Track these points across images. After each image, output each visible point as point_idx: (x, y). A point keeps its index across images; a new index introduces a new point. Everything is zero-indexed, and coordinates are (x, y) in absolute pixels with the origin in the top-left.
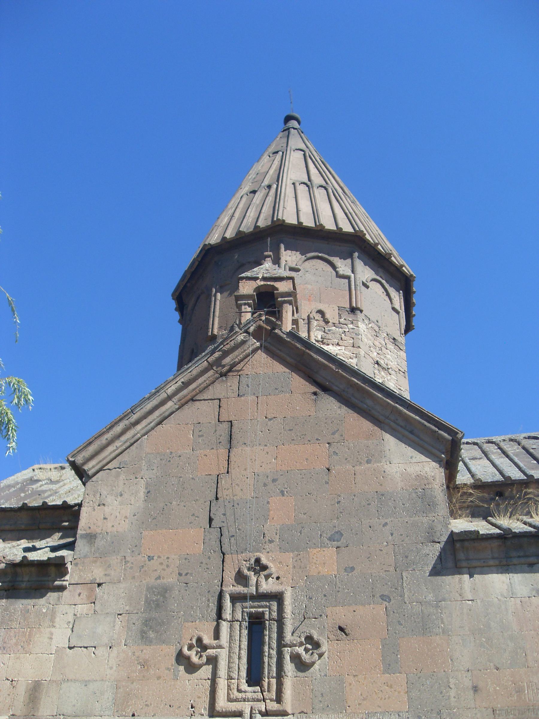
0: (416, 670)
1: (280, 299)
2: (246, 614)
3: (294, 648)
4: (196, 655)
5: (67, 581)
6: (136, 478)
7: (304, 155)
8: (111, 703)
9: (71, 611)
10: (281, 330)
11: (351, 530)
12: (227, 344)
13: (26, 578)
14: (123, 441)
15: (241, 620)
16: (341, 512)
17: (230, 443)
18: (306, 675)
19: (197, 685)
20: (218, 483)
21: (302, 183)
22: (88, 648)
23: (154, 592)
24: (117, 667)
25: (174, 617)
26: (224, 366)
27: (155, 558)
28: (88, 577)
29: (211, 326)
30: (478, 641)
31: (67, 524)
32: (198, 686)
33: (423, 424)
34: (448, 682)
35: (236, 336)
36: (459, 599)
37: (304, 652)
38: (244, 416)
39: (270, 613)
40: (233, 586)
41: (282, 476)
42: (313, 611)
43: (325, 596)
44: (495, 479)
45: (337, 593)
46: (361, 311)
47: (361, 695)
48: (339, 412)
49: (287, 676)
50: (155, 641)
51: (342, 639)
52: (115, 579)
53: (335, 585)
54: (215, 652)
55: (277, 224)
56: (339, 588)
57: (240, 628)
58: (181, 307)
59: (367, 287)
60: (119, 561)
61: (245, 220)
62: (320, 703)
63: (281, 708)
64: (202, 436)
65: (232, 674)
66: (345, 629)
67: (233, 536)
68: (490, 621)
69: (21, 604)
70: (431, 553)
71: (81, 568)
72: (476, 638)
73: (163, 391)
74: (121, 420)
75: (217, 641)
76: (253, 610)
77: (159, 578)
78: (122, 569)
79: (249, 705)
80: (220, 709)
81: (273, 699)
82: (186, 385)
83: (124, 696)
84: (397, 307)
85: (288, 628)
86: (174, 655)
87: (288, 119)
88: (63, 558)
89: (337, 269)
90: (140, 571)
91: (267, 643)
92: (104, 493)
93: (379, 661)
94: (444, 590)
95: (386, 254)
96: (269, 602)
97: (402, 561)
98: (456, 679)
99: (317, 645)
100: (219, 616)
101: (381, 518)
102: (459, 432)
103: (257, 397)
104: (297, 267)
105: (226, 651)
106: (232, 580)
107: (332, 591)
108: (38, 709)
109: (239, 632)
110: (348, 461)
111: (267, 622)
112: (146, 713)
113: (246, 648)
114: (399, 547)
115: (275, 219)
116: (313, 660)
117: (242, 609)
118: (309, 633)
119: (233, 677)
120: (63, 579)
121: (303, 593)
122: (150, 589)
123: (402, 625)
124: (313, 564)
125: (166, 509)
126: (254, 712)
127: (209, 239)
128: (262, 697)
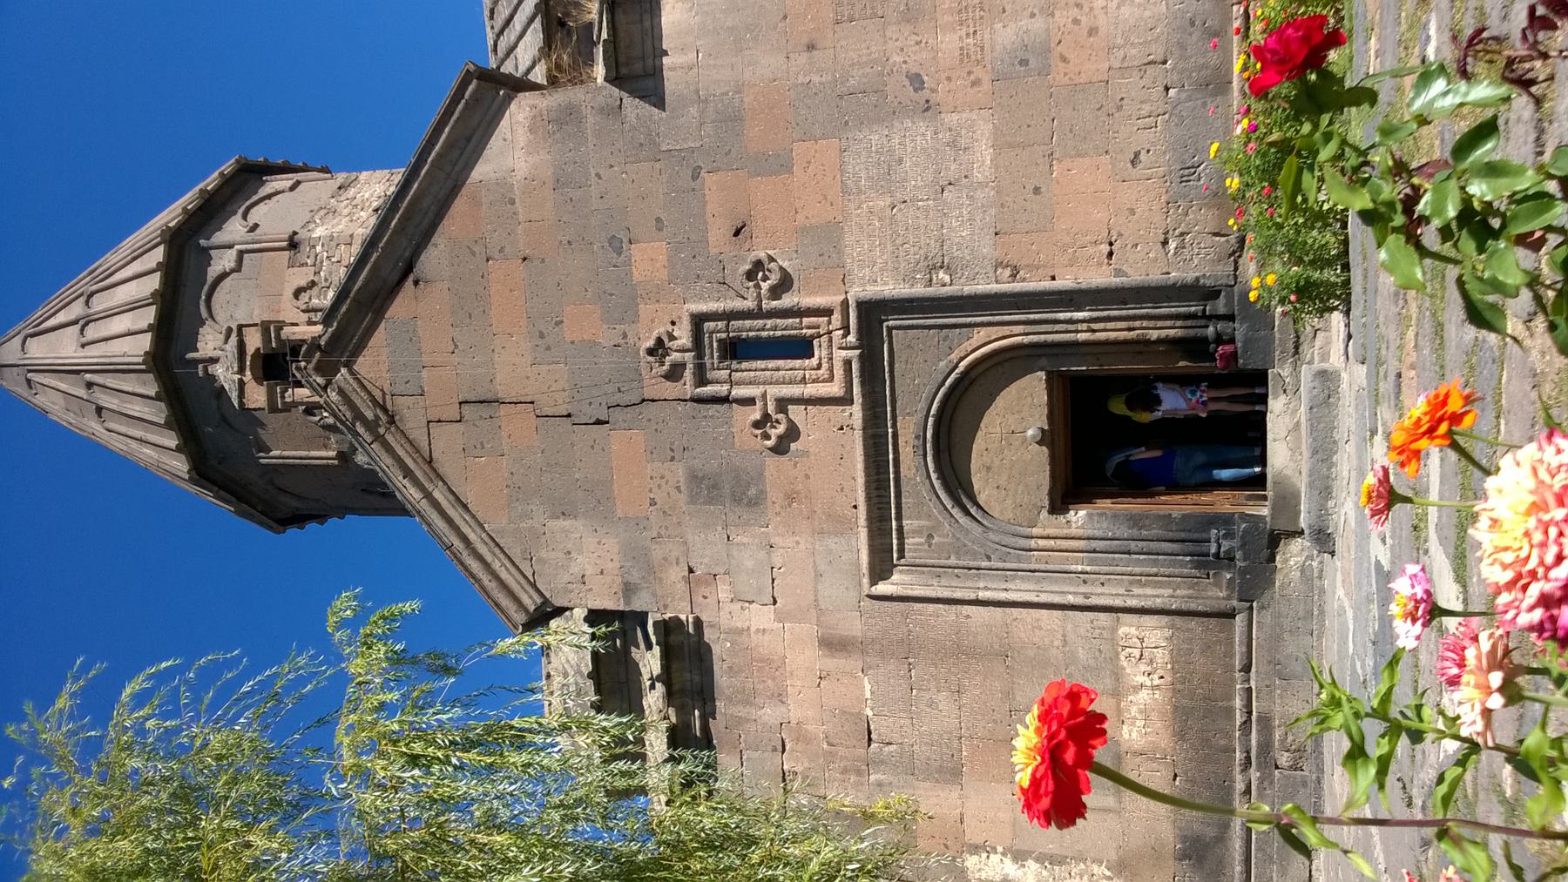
1: (274, 345)
5: (687, 617)
7: (32, 336)
10: (320, 337)
13: (688, 675)
16: (583, 239)
20: (547, 416)
21: (82, 334)
26: (377, 417)
28: (681, 587)
31: (618, 641)
33: (456, 122)
37: (768, 282)
39: (719, 332)
40: (685, 384)
43: (694, 257)
44: (540, 28)
46: (295, 233)
50: (761, 487)
55: (152, 364)
58: (299, 519)
59: (256, 226)
64: (482, 443)
65: (799, 379)
69: (722, 679)
76: (716, 355)
77: (678, 488)
82: (408, 473)
84: (289, 184)
85: (739, 304)
86: (777, 457)
88: (655, 624)
89: (227, 270)
92: (566, 578)
99: (758, 265)
100: (725, 400)
104: (224, 332)
108: (854, 637)
111: (731, 335)
115: (143, 367)
122: (693, 500)
126: (844, 345)
127: (180, 474)
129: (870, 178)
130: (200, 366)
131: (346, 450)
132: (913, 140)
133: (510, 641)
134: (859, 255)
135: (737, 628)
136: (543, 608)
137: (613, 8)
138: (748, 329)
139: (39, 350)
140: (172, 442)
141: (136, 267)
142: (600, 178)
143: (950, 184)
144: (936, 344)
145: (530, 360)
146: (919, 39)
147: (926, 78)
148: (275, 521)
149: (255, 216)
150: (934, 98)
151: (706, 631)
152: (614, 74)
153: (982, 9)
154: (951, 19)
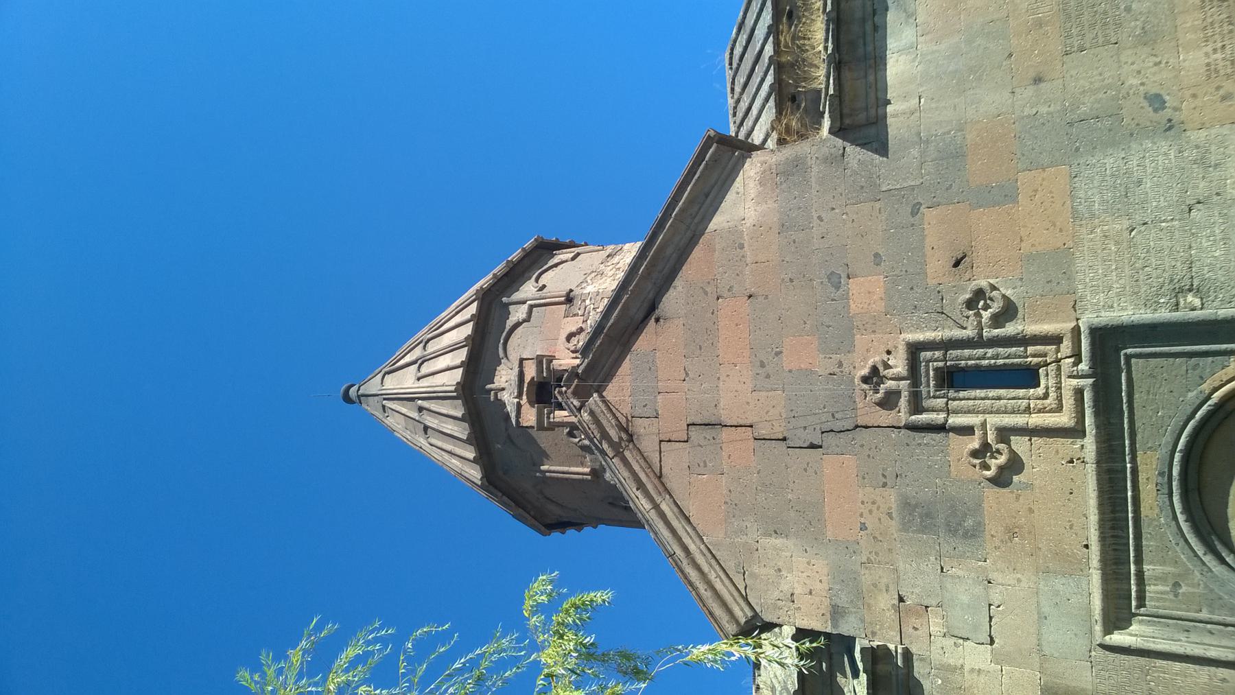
1: (545, 375)
2: (938, 393)
3: (983, 324)
4: (996, 459)
5: (896, 647)
6: (757, 550)
7: (389, 373)
9: (939, 642)
10: (578, 366)
11: (827, 261)
12: (593, 433)
15: (946, 399)
16: (804, 276)
17: (715, 425)
19: (1040, 456)
20: (764, 439)
22: (991, 615)
23: (909, 521)
24: (1017, 573)
28: (891, 615)
29: (581, 476)
30: (974, 85)
31: (824, 664)
33: (697, 180)
34: (1029, 116)
35: (583, 422)
37: (989, 310)
39: (936, 360)
40: (899, 412)
43: (912, 289)
46: (571, 291)
48: (680, 288)
50: (979, 518)
55: (461, 392)
56: (901, 270)
57: (958, 400)
58: (562, 525)
59: (544, 286)
60: (867, 572)
61: (456, 434)
63: (1069, 335)
64: (705, 462)
65: (1022, 408)
67: (833, 415)
70: (858, 157)
72: (970, 87)
73: (647, 515)
76: (932, 383)
77: (890, 515)
78: (878, 567)
79: (1065, 382)
82: (640, 486)
83: (1059, 561)
84: (571, 255)
85: (957, 333)
86: (997, 489)
87: (347, 398)
88: (863, 650)
89: (520, 320)
91: (978, 361)
92: (776, 594)
99: (979, 293)
100: (941, 428)
103: (659, 393)
105: (990, 417)
114: (848, 199)
115: (455, 394)
116: (1000, 297)
117: (930, 398)
119: (1027, 406)
120: (894, 654)
121: (909, 318)
122: (905, 527)
124: (870, 308)
126: (1075, 373)
127: (475, 481)
128: (1053, 364)
129: (1103, 202)
130: (492, 393)
131: (597, 467)
132: (1153, 161)
133: (705, 648)
136: (753, 622)
137: (840, 67)
138: (967, 358)
139: (393, 384)
140: (471, 455)
142: (822, 221)
143: (1199, 203)
144: (1184, 373)
145: (750, 386)
146: (1158, 60)
147: (1167, 98)
148: (544, 526)
150: (1177, 117)
151: (916, 664)
152: (838, 124)
153: (1231, 24)
154: (1193, 36)
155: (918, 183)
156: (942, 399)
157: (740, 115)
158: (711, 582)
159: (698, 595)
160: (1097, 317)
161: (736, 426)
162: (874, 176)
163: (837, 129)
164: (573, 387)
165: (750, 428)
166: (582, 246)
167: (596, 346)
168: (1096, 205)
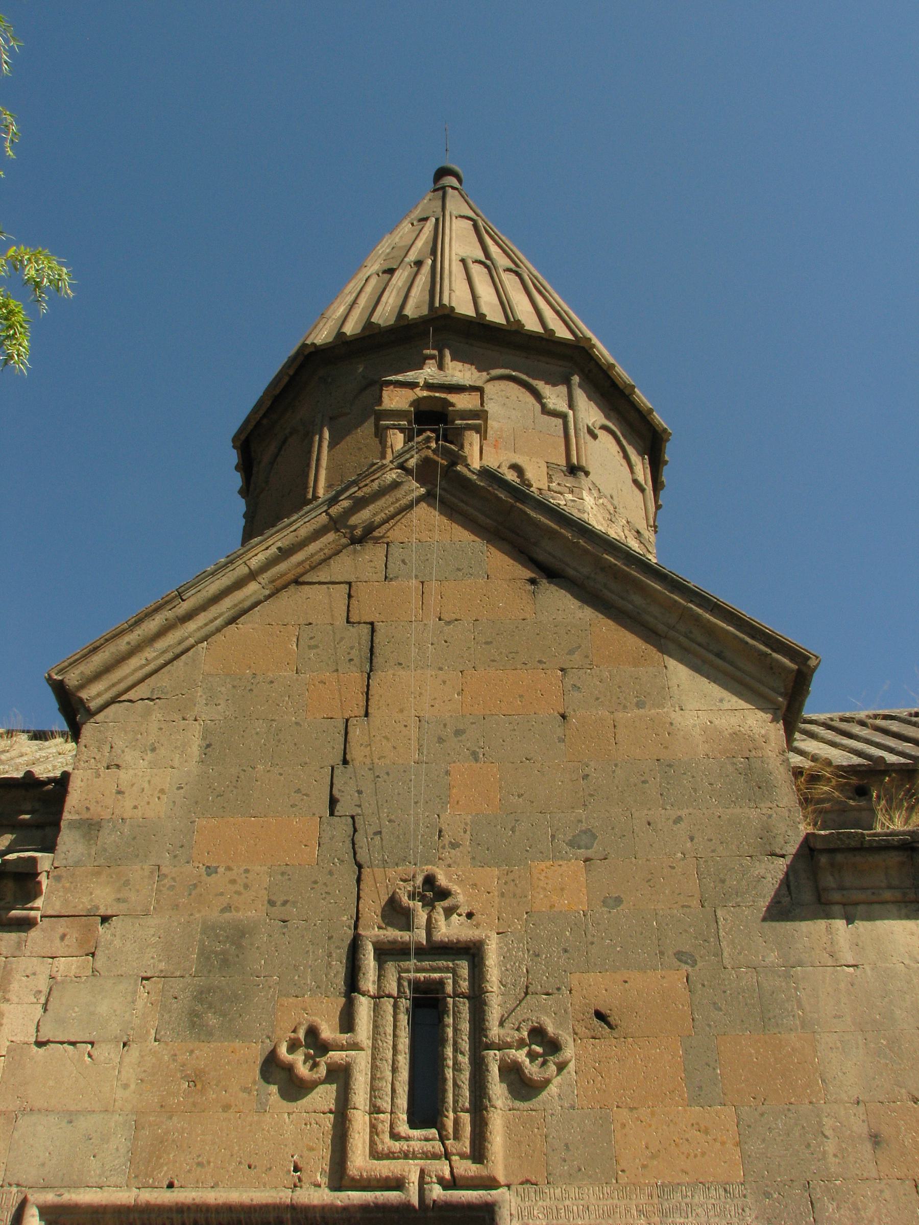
0: (754, 1098)
1: (457, 422)
2: (406, 984)
3: (508, 1050)
4: (305, 1062)
5: (37, 909)
6: (184, 719)
8: (122, 1160)
9: (43, 969)
10: (467, 466)
11: (613, 828)
12: (366, 485)
14: (160, 649)
15: (396, 995)
16: (591, 795)
17: (371, 663)
18: (531, 1106)
19: (306, 1124)
20: (346, 733)
23: (217, 936)
24: (137, 1084)
25: (259, 985)
27: (221, 870)
28: (82, 903)
29: (312, 484)
30: (872, 1045)
32: (309, 1126)
33: (742, 640)
34: (820, 1124)
35: (382, 472)
36: (830, 962)
37: (528, 1060)
38: (397, 615)
39: (455, 982)
40: (380, 928)
41: (474, 725)
42: (542, 979)
43: (566, 951)
45: (590, 946)
46: (587, 474)
47: (647, 1148)
48: (579, 614)
49: (496, 1108)
51: (602, 1035)
52: (139, 909)
53: (585, 931)
54: (345, 1056)
55: (440, 313)
56: (594, 936)
58: (247, 466)
59: (595, 437)
60: (147, 873)
61: (379, 309)
62: (563, 1163)
63: (485, 1173)
64: (317, 647)
65: (379, 1102)
66: (609, 1016)
68: (893, 1007)
70: (769, 875)
71: (68, 885)
73: (241, 562)
74: (157, 610)
75: (349, 1034)
76: (421, 976)
77: (227, 908)
78: (152, 889)
79: (417, 1165)
80: (356, 1173)
81: (467, 1153)
82: (285, 553)
83: (152, 1145)
84: (641, 479)
85: (494, 1013)
86: (259, 1061)
87: (442, 172)
88: (34, 860)
90: (190, 895)
91: (451, 1041)
92: (119, 744)
93: (678, 1080)
94: (800, 946)
95: (626, 387)
96: (453, 961)
97: (715, 888)
98: (836, 1118)
99: (553, 1046)
100: (352, 985)
101: (668, 808)
102: (811, 656)
103: (422, 583)
105: (367, 1055)
106: (377, 916)
107: (580, 942)
109: (392, 1019)
110: (601, 702)
111: (450, 1000)
112: (197, 1181)
113: (407, 1051)
115: (437, 304)
116: (546, 1076)
117: (399, 973)
118: (537, 1023)
119: (382, 1108)
120: (29, 905)
121: (521, 945)
122: (209, 929)
123: (720, 1010)
125: (243, 777)
126: (428, 1179)
127: (312, 337)
128: (442, 1149)
130: (436, 352)
134: (567, 1208)
135: (10, 983)
141: (548, 314)
149: (605, 439)
151: (13, 936)
152: (819, 846)
155: (726, 962)
156: (396, 989)
157: (844, 726)
158: (138, 652)
159: (122, 633)
160: (511, 1215)
161: (367, 694)
162: (739, 899)
163: (812, 845)
164: (435, 458)
165: (363, 712)
166: (656, 501)
167: (496, 492)
168: (682, 1220)
